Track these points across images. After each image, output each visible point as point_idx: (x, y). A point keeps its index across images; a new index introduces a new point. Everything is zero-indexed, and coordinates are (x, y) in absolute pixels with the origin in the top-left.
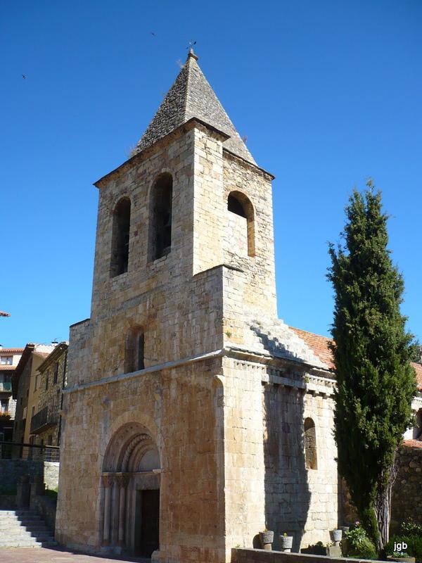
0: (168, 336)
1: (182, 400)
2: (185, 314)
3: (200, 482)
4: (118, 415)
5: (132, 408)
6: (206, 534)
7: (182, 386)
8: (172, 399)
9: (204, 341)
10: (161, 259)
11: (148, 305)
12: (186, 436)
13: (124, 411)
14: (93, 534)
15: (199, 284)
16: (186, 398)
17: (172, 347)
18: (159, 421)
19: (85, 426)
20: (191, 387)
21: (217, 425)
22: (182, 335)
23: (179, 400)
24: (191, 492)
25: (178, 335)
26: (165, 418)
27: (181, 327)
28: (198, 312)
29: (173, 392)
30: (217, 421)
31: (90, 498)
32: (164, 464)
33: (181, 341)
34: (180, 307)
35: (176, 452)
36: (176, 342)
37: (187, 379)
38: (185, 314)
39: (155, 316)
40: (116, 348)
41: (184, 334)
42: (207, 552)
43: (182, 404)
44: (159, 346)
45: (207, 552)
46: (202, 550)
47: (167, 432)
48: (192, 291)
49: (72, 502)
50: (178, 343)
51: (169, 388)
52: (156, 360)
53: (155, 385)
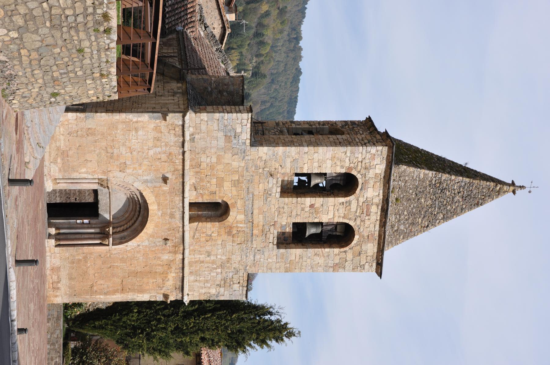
0: (208, 248)
1: (159, 265)
2: (222, 266)
3: (102, 282)
4: (156, 197)
5: (160, 213)
6: (69, 288)
7: (169, 265)
8: (160, 255)
9: (197, 284)
10: (276, 238)
11: (241, 225)
12: (133, 269)
13: (159, 205)
14: (60, 170)
15: (241, 278)
16: (159, 269)
17: (200, 253)
18: (146, 243)
19: (151, 152)
20: (167, 273)
21: (138, 295)
22: (207, 263)
23: (160, 262)
24: (96, 275)
25: (208, 259)
26: (148, 249)
27: (213, 262)
28: (219, 277)
29: (166, 257)
30: (141, 295)
31: (89, 164)
32: (115, 249)
33: (203, 262)
34: (229, 260)
35: (123, 260)
36: (202, 257)
37: (173, 269)
38: (222, 266)
39: (229, 233)
40: (213, 188)
41: (206, 265)
42: (58, 288)
43: (156, 265)
44: (204, 239)
45: (58, 288)
46: (59, 285)
47: (137, 252)
48: (237, 272)
49: (84, 139)
50: (201, 259)
51: (170, 252)
52: (194, 236)
53: (174, 239)
